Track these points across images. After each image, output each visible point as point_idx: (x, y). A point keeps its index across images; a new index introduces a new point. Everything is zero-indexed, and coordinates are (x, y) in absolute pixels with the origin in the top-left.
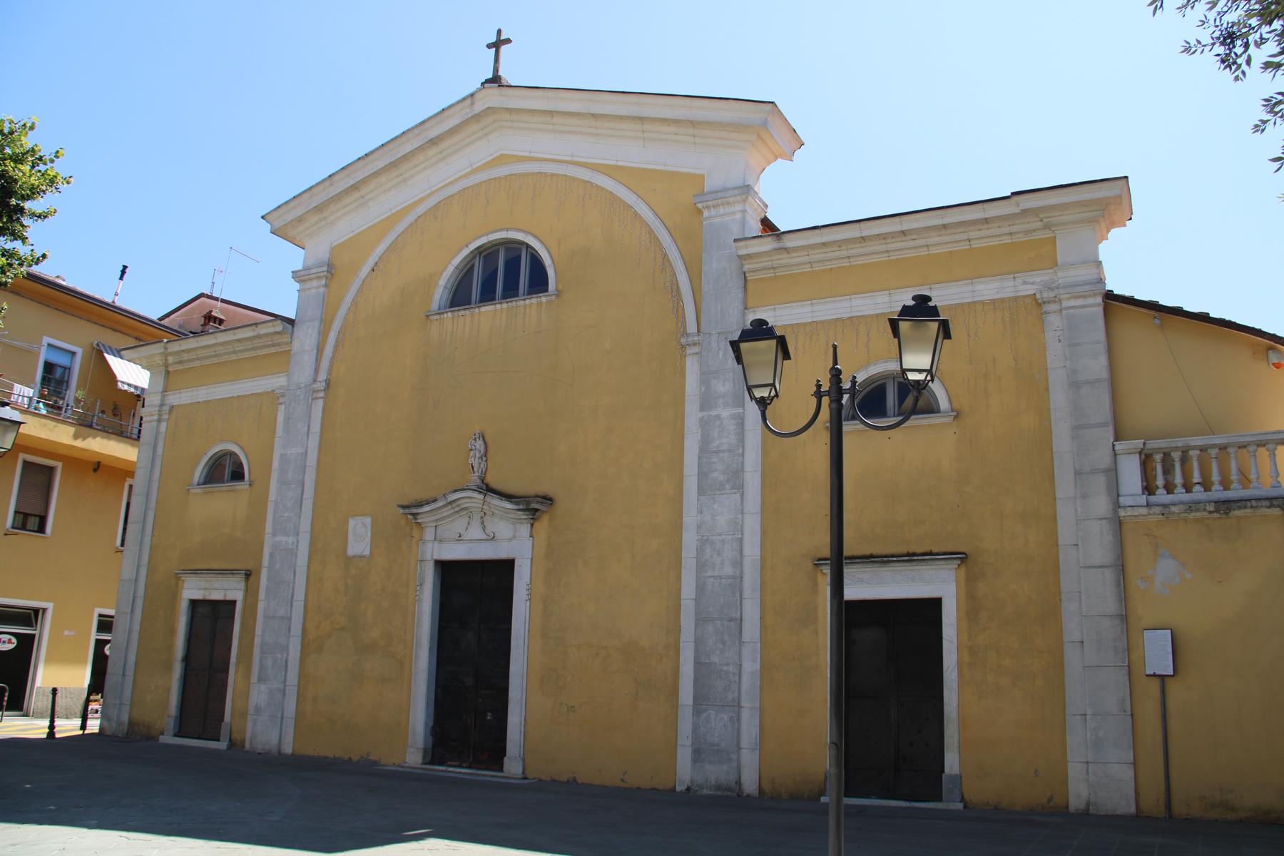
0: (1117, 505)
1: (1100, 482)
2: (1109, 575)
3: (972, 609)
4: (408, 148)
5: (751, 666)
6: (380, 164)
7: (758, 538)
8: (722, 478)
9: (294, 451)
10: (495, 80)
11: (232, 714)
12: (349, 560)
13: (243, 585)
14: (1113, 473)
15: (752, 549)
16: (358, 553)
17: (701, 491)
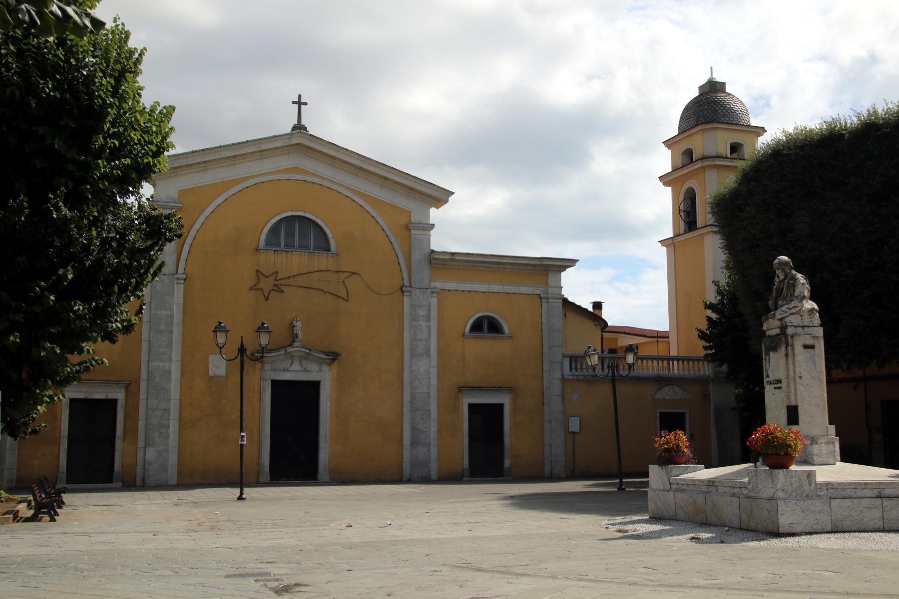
0: (563, 375)
3: (514, 410)
5: (434, 429)
6: (228, 154)
7: (436, 377)
9: (164, 313)
10: (299, 127)
11: (123, 467)
13: (123, 390)
14: (562, 363)
15: (434, 382)
16: (218, 374)
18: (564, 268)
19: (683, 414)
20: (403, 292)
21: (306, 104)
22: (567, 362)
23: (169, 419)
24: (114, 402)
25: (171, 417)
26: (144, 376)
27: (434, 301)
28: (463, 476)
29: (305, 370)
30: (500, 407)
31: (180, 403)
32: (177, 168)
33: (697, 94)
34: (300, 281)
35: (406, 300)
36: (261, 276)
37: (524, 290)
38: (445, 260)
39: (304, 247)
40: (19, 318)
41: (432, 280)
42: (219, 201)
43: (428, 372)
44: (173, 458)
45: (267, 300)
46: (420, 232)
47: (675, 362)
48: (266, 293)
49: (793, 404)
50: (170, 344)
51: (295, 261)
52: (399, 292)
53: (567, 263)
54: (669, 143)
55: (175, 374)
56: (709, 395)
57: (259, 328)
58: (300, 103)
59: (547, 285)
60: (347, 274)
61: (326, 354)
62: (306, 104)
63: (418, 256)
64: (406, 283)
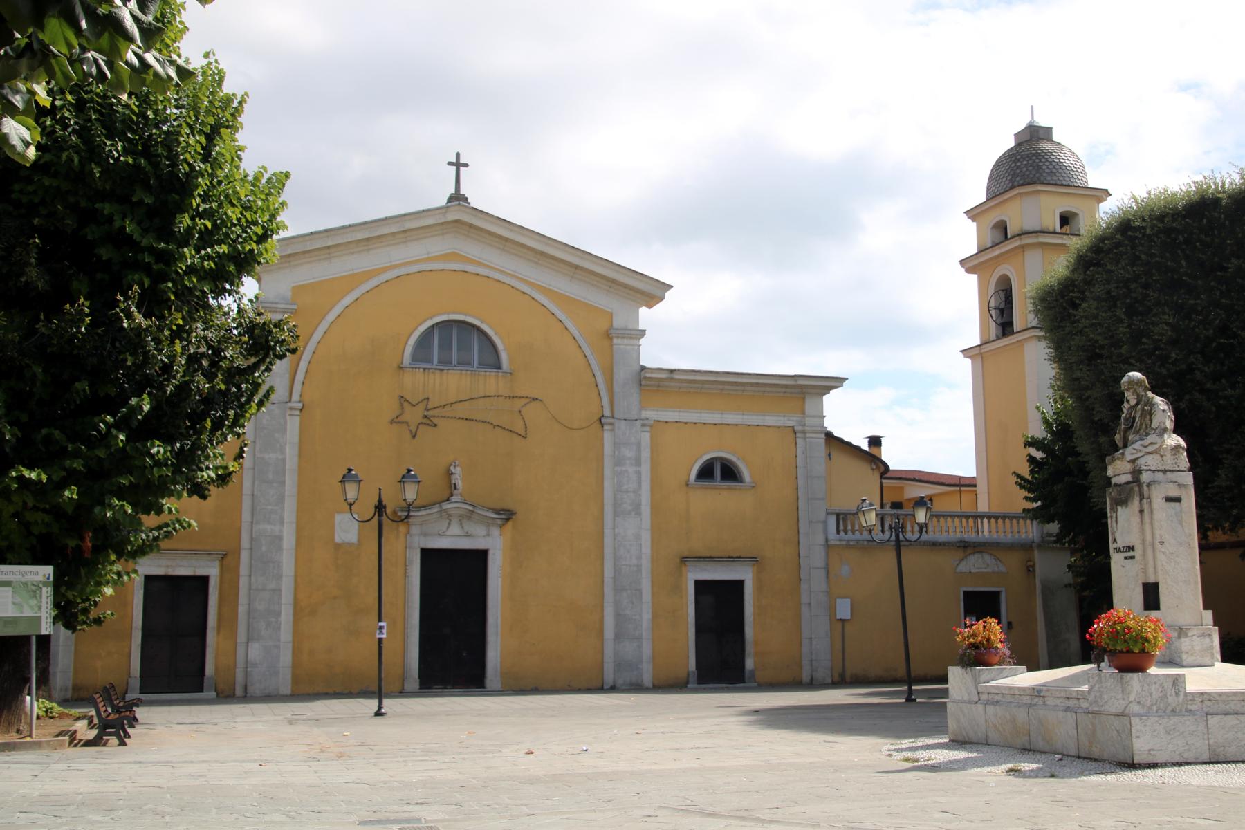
0: (827, 540)
1: (820, 526)
2: (823, 573)
3: (759, 588)
4: (386, 230)
5: (647, 616)
6: (360, 236)
7: (649, 543)
8: (630, 508)
10: (457, 198)
11: (216, 669)
12: (338, 546)
13: (217, 564)
14: (825, 522)
15: (647, 550)
17: (616, 514)
18: (827, 389)
19: (997, 594)
20: (602, 425)
21: (466, 165)
22: (832, 521)
23: (280, 604)
24: (205, 580)
25: (283, 601)
26: (245, 543)
27: (646, 437)
28: (688, 683)
29: (468, 535)
30: (739, 585)
31: (296, 581)
32: (289, 256)
33: (1012, 144)
34: (460, 410)
35: (607, 436)
36: (406, 404)
37: (770, 420)
38: (660, 379)
39: (465, 363)
40: (78, 465)
41: (642, 408)
42: (347, 300)
43: (638, 537)
44: (286, 658)
45: (414, 437)
46: (625, 341)
47: (985, 521)
48: (413, 429)
49: (1152, 580)
50: (281, 499)
51: (452, 383)
52: (598, 425)
53: (835, 382)
54: (973, 214)
55: (289, 540)
56: (1033, 566)
57: (403, 477)
58: (458, 165)
59: (803, 413)
60: (524, 401)
61: (497, 512)
62: (466, 165)
63: (623, 374)
64: (607, 413)
